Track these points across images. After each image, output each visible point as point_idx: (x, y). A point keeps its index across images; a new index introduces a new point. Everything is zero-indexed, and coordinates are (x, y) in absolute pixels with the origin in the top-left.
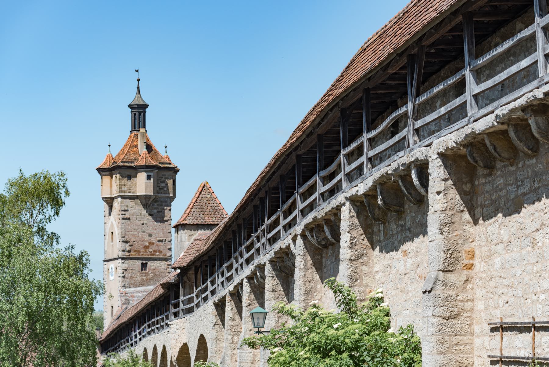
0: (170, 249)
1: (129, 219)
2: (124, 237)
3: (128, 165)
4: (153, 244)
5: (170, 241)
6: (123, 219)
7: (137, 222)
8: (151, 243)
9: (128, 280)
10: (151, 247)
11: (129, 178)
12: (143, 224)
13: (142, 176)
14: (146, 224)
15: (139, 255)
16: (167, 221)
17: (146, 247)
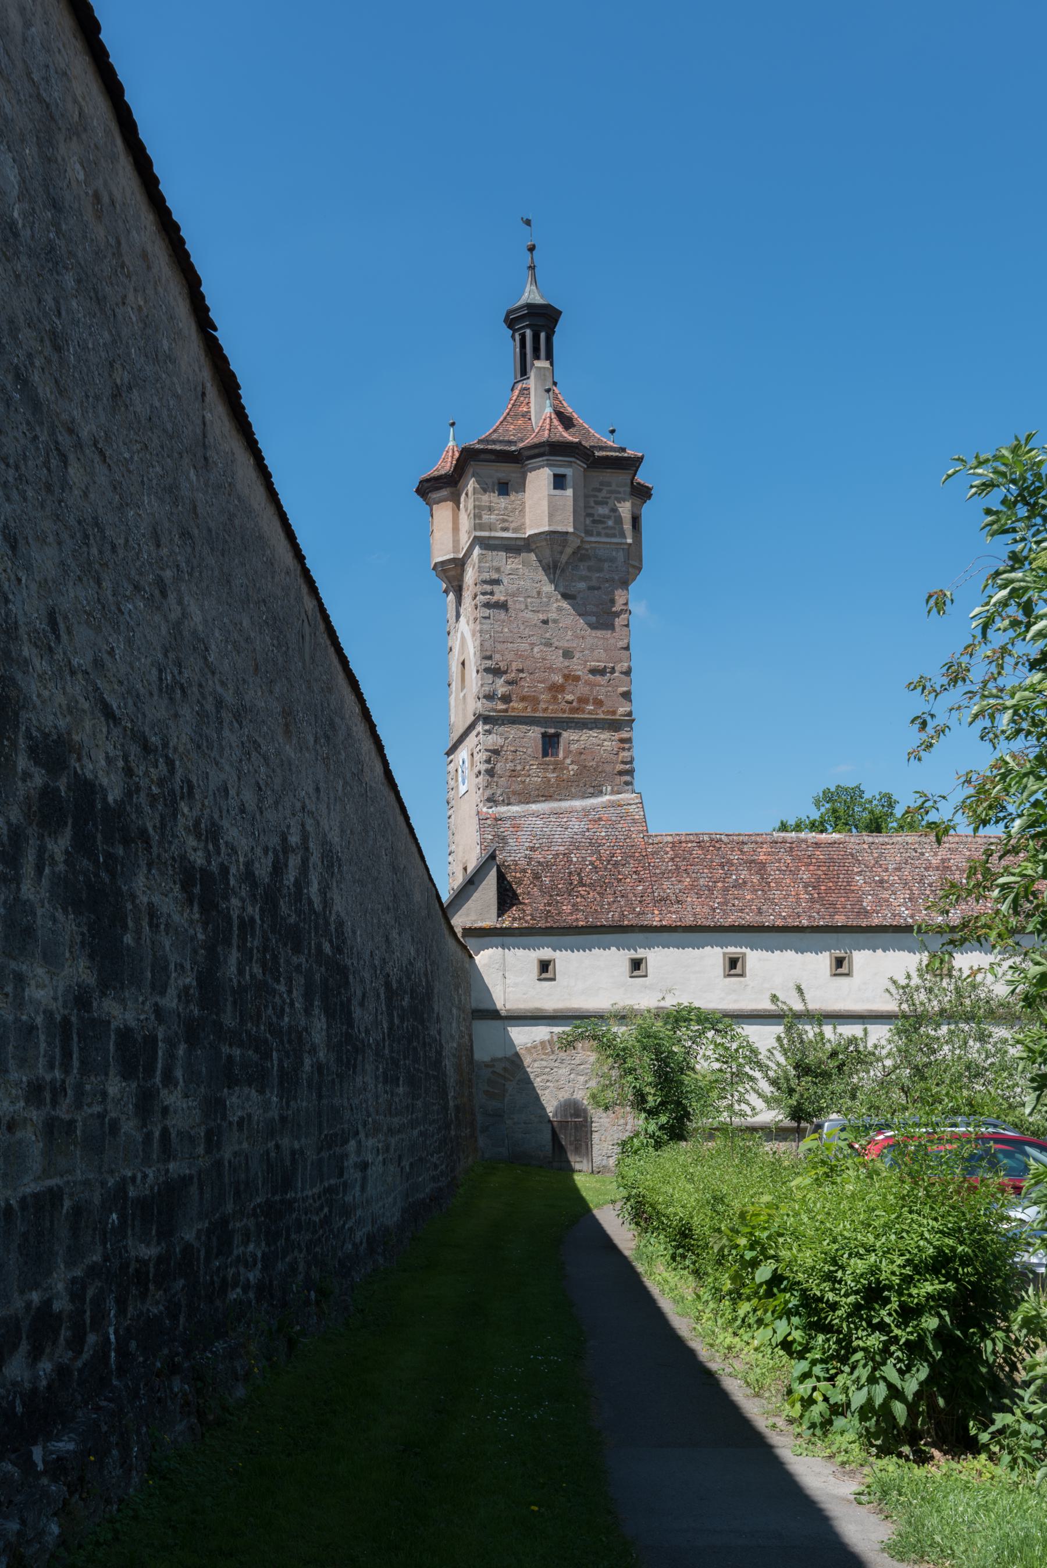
0: (627, 696)
1: (503, 606)
2: (490, 658)
3: (498, 447)
4: (577, 679)
5: (628, 673)
6: (487, 605)
7: (529, 615)
8: (571, 678)
9: (503, 781)
10: (569, 688)
11: (504, 488)
12: (545, 622)
13: (539, 480)
14: (555, 621)
15: (535, 710)
16: (618, 614)
17: (556, 689)
